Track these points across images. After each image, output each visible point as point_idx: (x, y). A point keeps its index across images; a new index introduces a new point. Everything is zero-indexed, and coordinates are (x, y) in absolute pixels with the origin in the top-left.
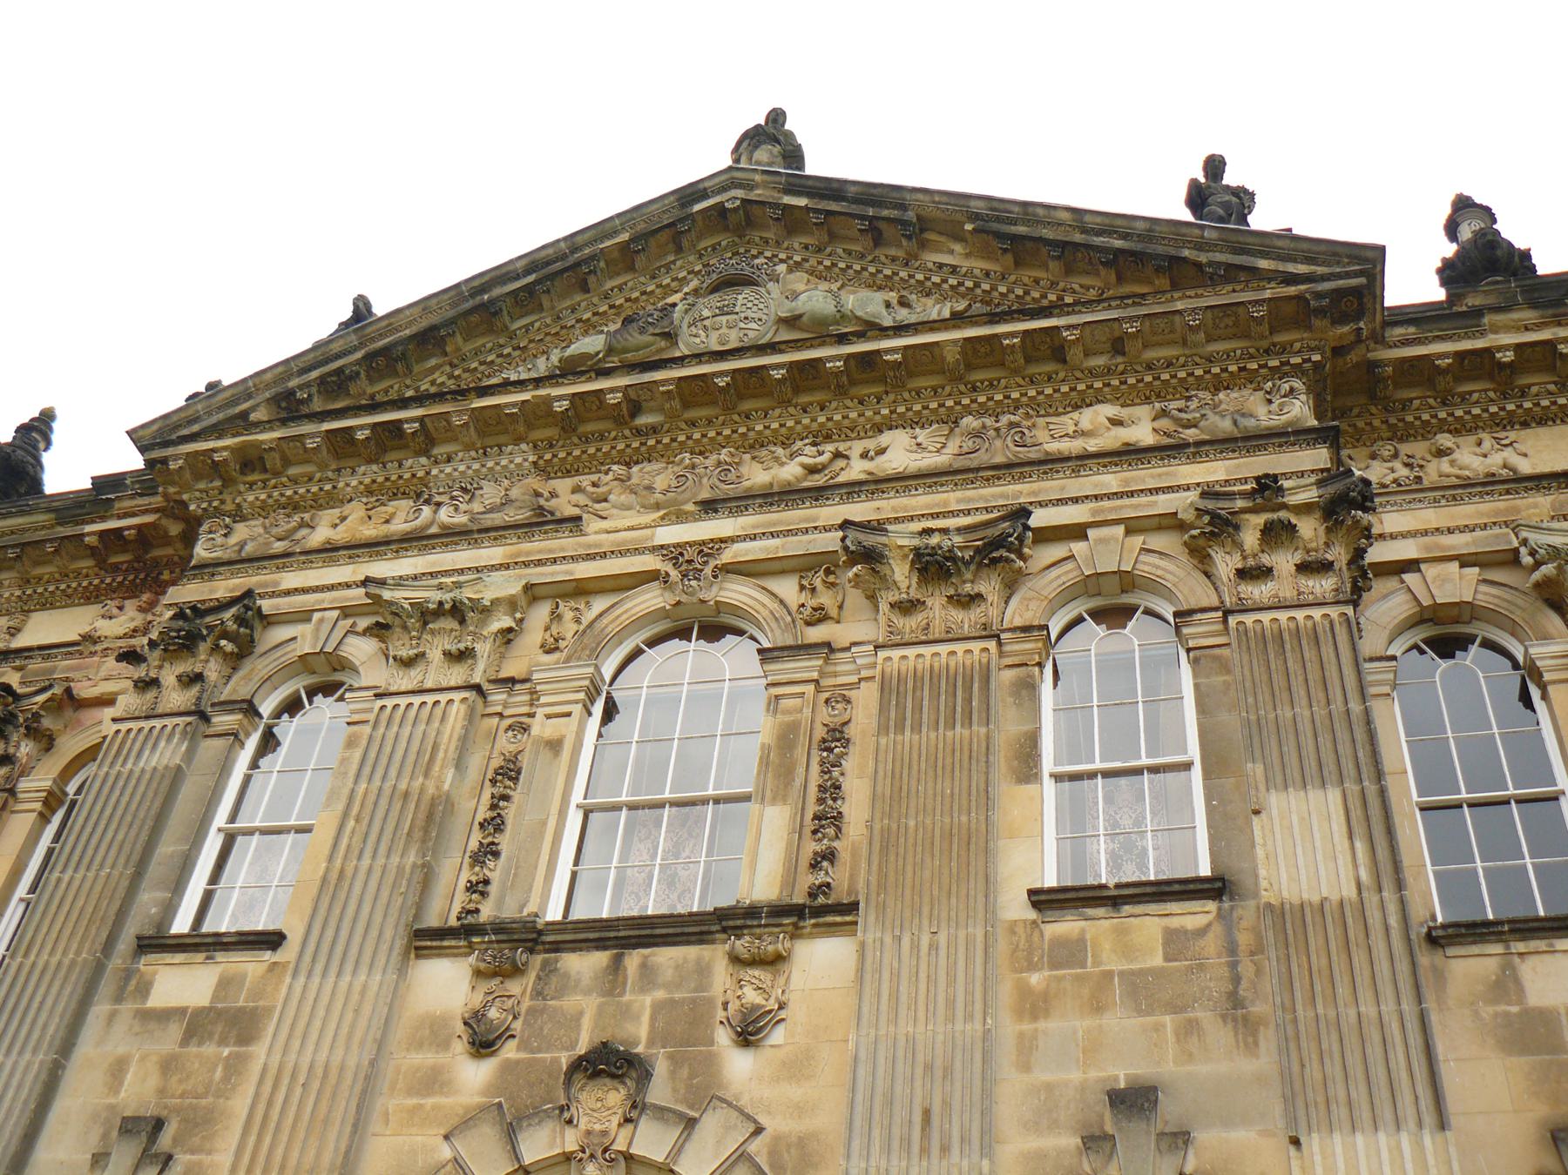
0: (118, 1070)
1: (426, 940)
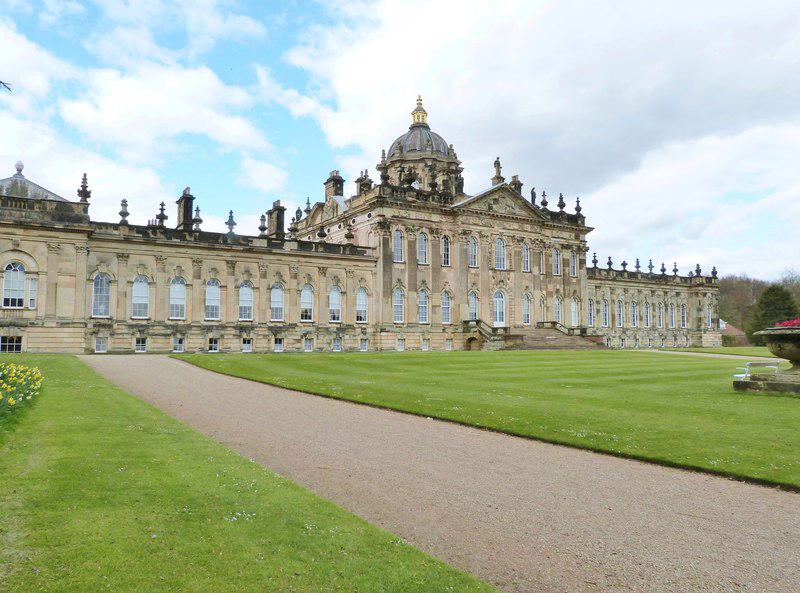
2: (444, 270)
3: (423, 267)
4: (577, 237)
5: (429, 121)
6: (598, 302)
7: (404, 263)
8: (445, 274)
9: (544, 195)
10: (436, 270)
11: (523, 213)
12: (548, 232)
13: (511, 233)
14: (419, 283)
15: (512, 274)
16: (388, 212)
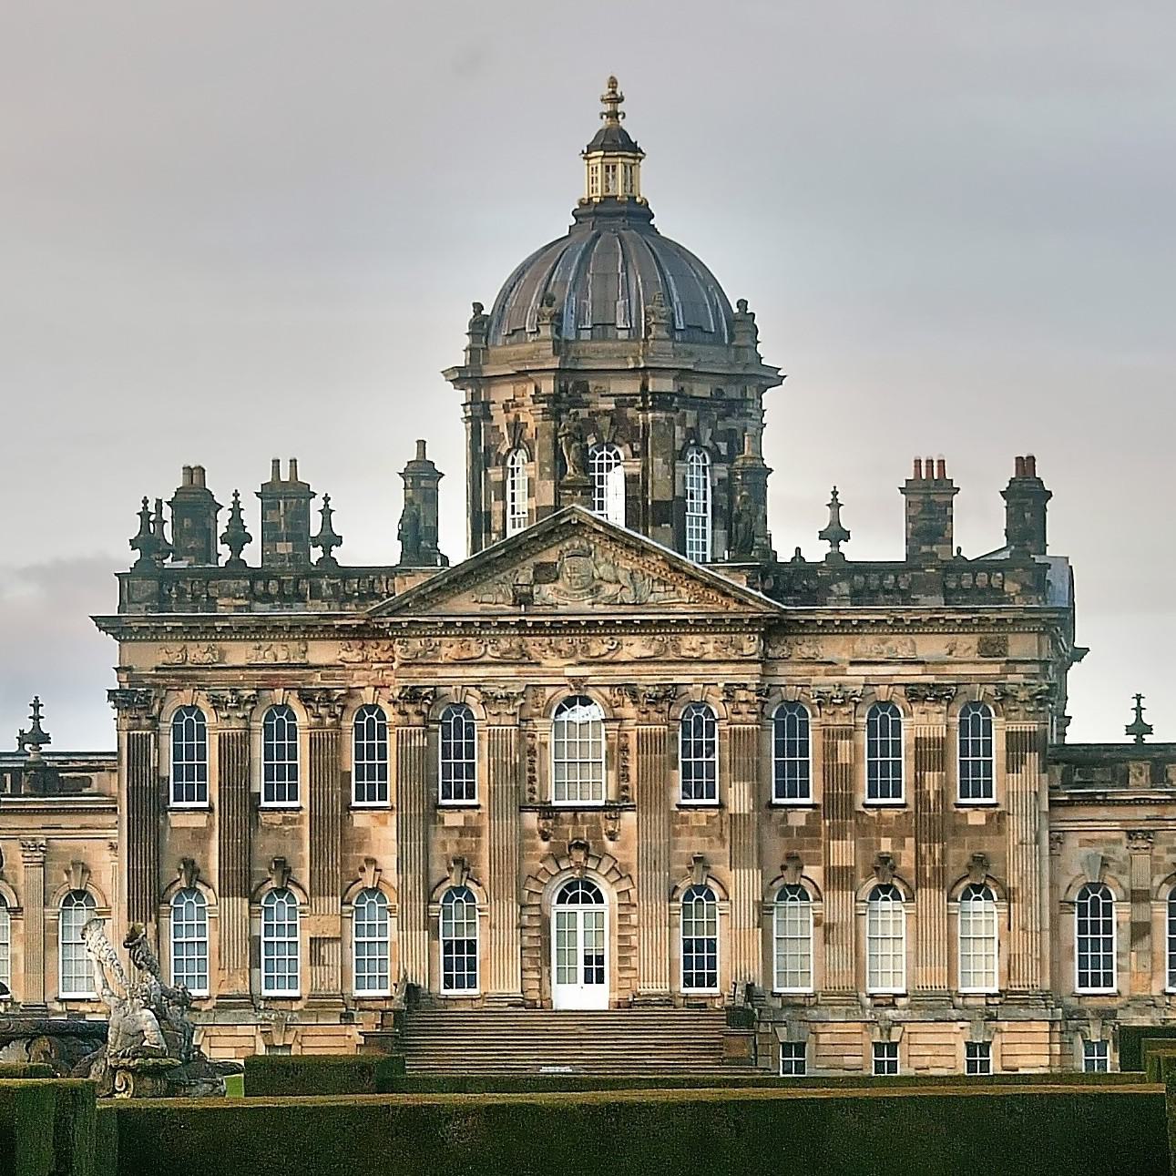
0: (444, 844)
1: (522, 809)
2: (360, 820)
3: (278, 817)
4: (989, 650)
5: (652, 185)
6: (1138, 897)
7: (211, 809)
8: (365, 832)
9: (835, 505)
10: (332, 827)
11: (682, 602)
12: (835, 648)
13: (621, 674)
14: (260, 868)
15: (629, 818)
16: (150, 657)
